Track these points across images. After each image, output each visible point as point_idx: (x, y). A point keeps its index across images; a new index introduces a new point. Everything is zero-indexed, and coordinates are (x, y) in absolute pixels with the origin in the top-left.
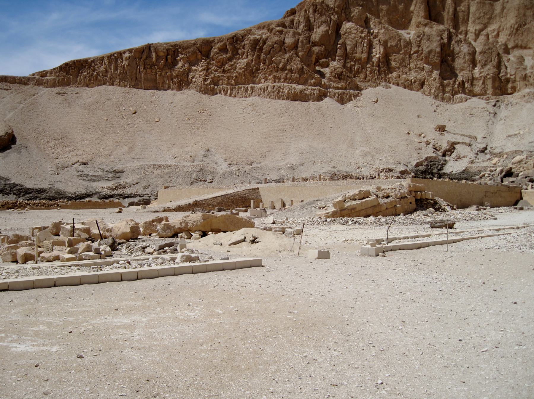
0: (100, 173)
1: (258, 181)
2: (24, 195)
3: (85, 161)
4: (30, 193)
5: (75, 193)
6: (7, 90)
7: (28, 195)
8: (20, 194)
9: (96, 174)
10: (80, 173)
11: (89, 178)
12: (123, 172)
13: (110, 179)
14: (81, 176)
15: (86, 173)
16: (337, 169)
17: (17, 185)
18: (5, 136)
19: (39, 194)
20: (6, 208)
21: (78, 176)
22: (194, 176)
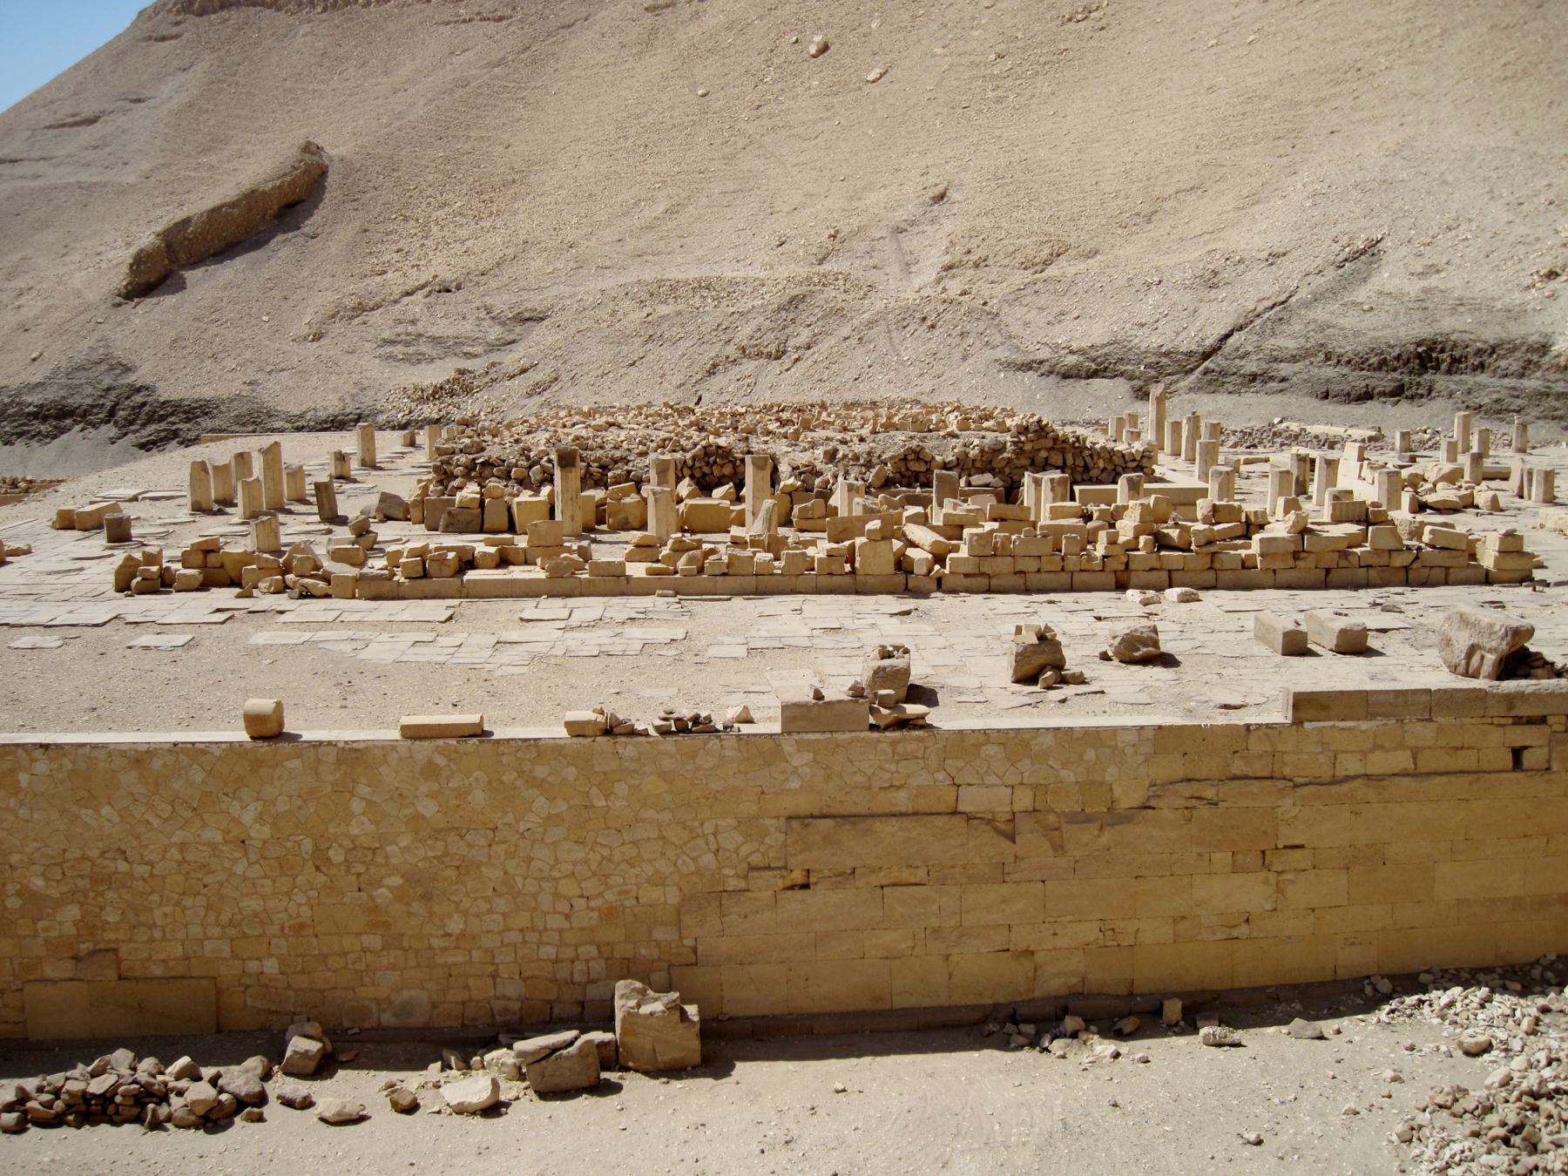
0: (467, 328)
1: (1002, 354)
2: (144, 425)
3: (447, 275)
4: (162, 419)
5: (302, 416)
6: (501, 19)
7: (152, 428)
8: (132, 423)
9: (451, 332)
10: (400, 329)
11: (411, 350)
12: (542, 319)
13: (478, 349)
14: (392, 342)
15: (420, 328)
16: (1433, 281)
17: (139, 390)
18: (233, 205)
19: (188, 420)
22: (744, 332)
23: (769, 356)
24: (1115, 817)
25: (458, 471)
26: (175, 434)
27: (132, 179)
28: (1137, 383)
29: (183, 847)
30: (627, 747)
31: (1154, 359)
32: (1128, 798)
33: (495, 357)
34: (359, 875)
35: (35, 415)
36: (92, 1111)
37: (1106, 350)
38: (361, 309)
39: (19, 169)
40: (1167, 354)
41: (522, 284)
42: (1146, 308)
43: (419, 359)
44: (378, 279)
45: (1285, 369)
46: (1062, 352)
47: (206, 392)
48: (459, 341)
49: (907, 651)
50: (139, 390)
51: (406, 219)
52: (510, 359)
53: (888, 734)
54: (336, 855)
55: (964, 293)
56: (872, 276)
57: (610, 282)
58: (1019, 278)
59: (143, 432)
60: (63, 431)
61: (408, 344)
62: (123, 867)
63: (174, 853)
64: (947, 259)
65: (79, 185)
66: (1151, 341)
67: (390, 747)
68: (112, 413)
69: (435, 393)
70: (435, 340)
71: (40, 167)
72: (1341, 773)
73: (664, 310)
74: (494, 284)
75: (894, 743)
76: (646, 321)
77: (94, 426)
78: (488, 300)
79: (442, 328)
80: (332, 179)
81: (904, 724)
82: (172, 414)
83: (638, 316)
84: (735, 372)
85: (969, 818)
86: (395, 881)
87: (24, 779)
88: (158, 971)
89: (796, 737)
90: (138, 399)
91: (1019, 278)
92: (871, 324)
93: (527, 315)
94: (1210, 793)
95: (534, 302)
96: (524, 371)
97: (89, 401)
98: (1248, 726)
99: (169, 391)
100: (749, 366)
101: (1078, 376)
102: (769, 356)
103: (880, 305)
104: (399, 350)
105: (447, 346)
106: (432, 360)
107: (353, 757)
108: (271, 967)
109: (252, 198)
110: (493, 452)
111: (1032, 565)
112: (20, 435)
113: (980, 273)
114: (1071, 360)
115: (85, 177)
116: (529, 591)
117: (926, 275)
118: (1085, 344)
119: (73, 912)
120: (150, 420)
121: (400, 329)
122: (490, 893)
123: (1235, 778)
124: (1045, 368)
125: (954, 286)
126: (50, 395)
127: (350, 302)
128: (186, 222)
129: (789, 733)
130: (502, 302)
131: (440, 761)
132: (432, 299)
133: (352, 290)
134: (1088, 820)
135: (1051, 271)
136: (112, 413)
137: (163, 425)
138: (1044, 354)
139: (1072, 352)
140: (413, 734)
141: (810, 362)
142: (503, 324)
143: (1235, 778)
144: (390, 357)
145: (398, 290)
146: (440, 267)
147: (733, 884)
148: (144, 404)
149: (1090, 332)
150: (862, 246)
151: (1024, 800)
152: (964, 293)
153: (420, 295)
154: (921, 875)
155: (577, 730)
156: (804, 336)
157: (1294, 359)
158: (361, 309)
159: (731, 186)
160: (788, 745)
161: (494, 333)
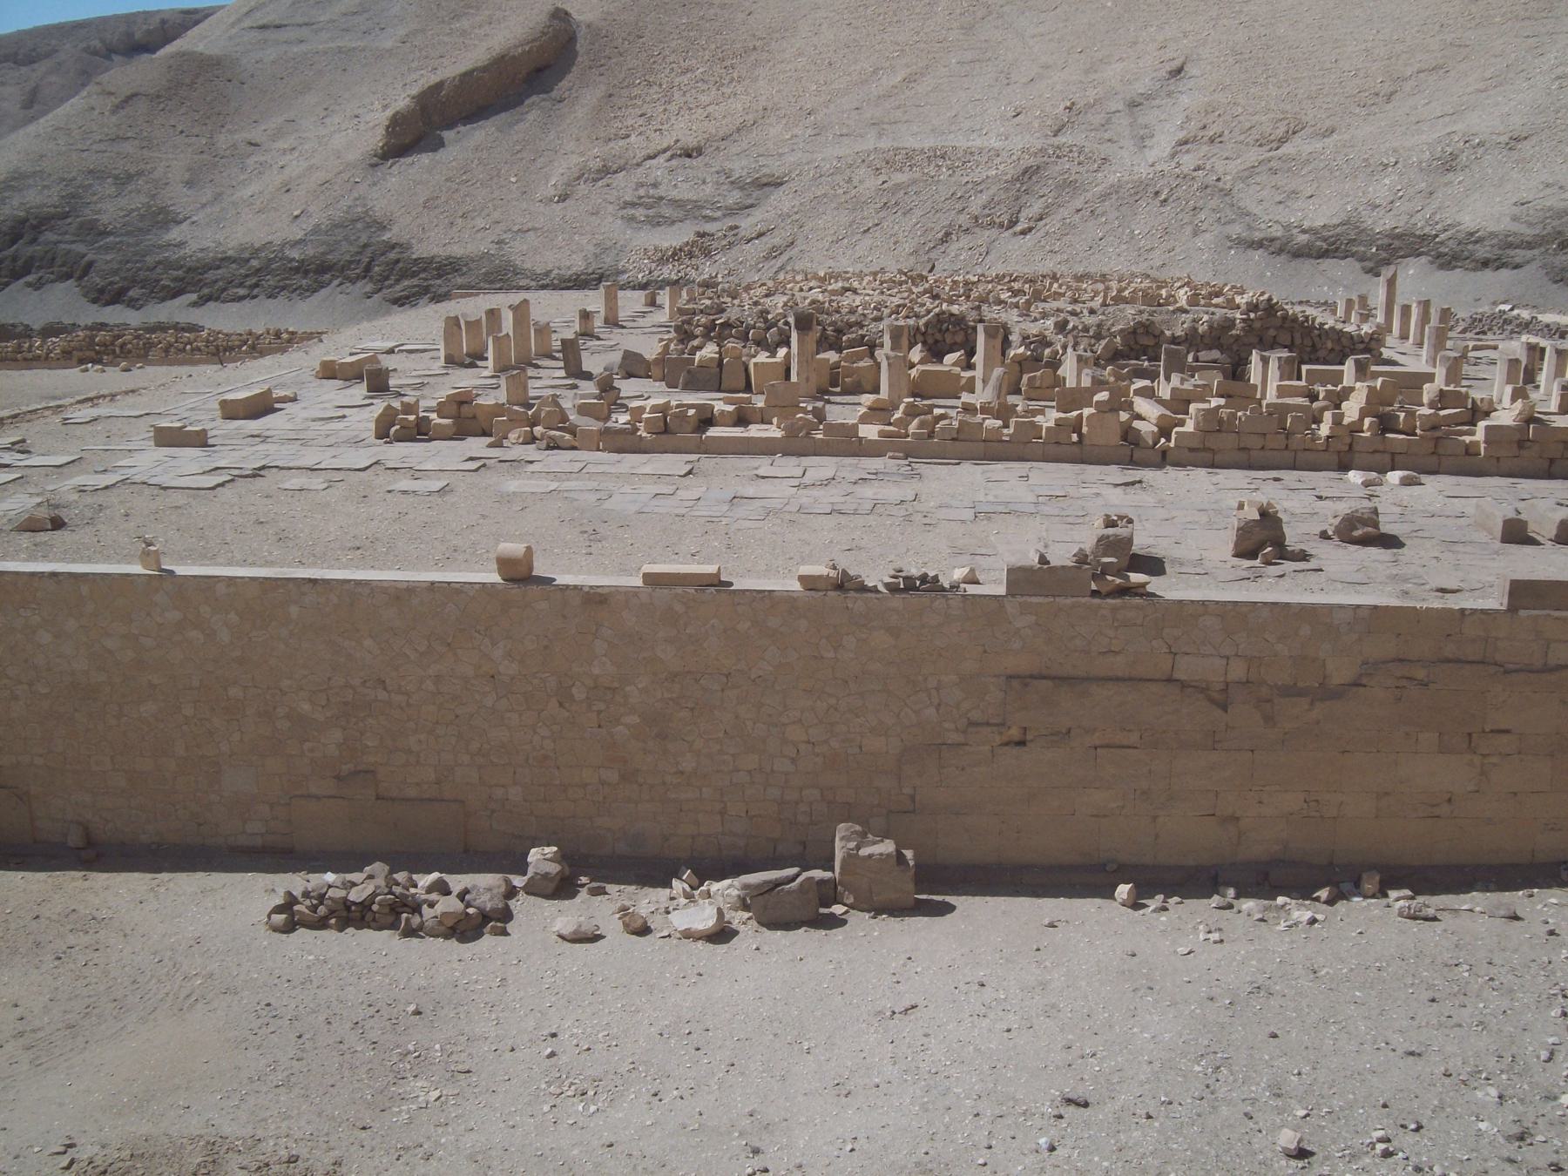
1: (1236, 230)
2: (398, 281)
3: (691, 141)
4: (414, 275)
5: (547, 274)
8: (387, 278)
9: (692, 196)
10: (642, 192)
11: (651, 212)
12: (781, 184)
14: (633, 205)
15: (661, 192)
17: (393, 247)
18: (484, 69)
19: (439, 276)
20: (75, 359)
21: (627, 205)
22: (976, 204)
23: (1001, 225)
24: (1328, 693)
25: (698, 331)
26: (426, 290)
27: (389, 44)
28: (1369, 264)
29: (438, 678)
30: (856, 602)
31: (1386, 241)
32: (1340, 672)
33: (730, 222)
34: (599, 712)
35: (297, 270)
36: (352, 916)
37: (1339, 230)
38: (605, 171)
39: (283, 35)
40: (1399, 237)
41: (761, 150)
42: (1382, 188)
43: (656, 222)
44: (621, 143)
45: (1520, 255)
46: (1295, 231)
47: (457, 251)
48: (697, 205)
49: (1130, 521)
50: (393, 247)
51: (650, 85)
52: (748, 224)
53: (1109, 601)
54: (579, 693)
55: (1197, 169)
56: (1106, 150)
57: (846, 149)
58: (1253, 155)
59: (398, 288)
60: (322, 286)
61: (649, 207)
62: (382, 695)
63: (429, 685)
64: (1181, 135)
65: (340, 50)
66: (1383, 223)
67: (633, 593)
68: (368, 269)
69: (674, 254)
70: (677, 203)
71: (305, 31)
72: (1552, 661)
73: (900, 178)
74: (734, 149)
75: (1114, 609)
76: (880, 191)
77: (353, 281)
78: (728, 165)
79: (684, 192)
80: (582, 46)
81: (1126, 591)
82: (424, 270)
83: (872, 183)
84: (965, 241)
85: (1184, 685)
86: (635, 719)
87: (294, 610)
88: (412, 793)
89: (1019, 599)
90: (392, 255)
91: (1253, 155)
92: (1105, 196)
93: (765, 180)
94: (1421, 674)
95: (774, 167)
96: (760, 235)
97: (348, 258)
98: (1462, 610)
99: (420, 251)
100: (983, 236)
101: (1309, 256)
102: (1001, 225)
103: (1113, 179)
104: (640, 213)
105: (689, 209)
106: (673, 222)
107: (596, 599)
108: (515, 793)
109: (501, 63)
110: (732, 314)
111: (1255, 442)
112: (283, 288)
113: (1215, 148)
114: (1303, 238)
115: (346, 42)
116: (765, 448)
117: (1162, 145)
118: (1319, 223)
119: (337, 735)
120: (404, 275)
121: (642, 192)
122: (721, 735)
123: (1449, 661)
124: (1277, 244)
125: (1188, 161)
126: (310, 251)
127: (596, 164)
128: (439, 86)
129: (1013, 596)
130: (740, 167)
131: (679, 608)
132: (674, 162)
133: (595, 155)
134: (1301, 693)
135: (1287, 149)
136: (368, 269)
137: (415, 281)
138: (1277, 231)
139: (1304, 232)
140: (652, 580)
141: (1042, 233)
142: (742, 189)
143: (1449, 661)
144: (632, 219)
145: (640, 155)
146: (683, 131)
147: (954, 737)
148: (398, 261)
149: (1320, 212)
150: (1097, 119)
151: (1238, 671)
152: (1197, 169)
153: (661, 159)
154: (1134, 738)
155: (809, 582)
156: (1036, 207)
157: (1530, 246)
158: (605, 171)
159: (969, 56)
160: (1011, 607)
161: (734, 197)
